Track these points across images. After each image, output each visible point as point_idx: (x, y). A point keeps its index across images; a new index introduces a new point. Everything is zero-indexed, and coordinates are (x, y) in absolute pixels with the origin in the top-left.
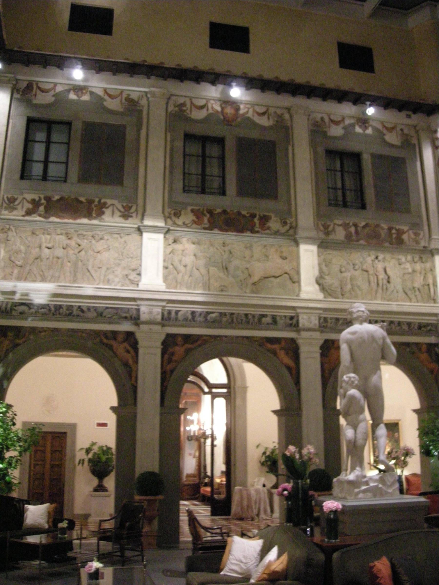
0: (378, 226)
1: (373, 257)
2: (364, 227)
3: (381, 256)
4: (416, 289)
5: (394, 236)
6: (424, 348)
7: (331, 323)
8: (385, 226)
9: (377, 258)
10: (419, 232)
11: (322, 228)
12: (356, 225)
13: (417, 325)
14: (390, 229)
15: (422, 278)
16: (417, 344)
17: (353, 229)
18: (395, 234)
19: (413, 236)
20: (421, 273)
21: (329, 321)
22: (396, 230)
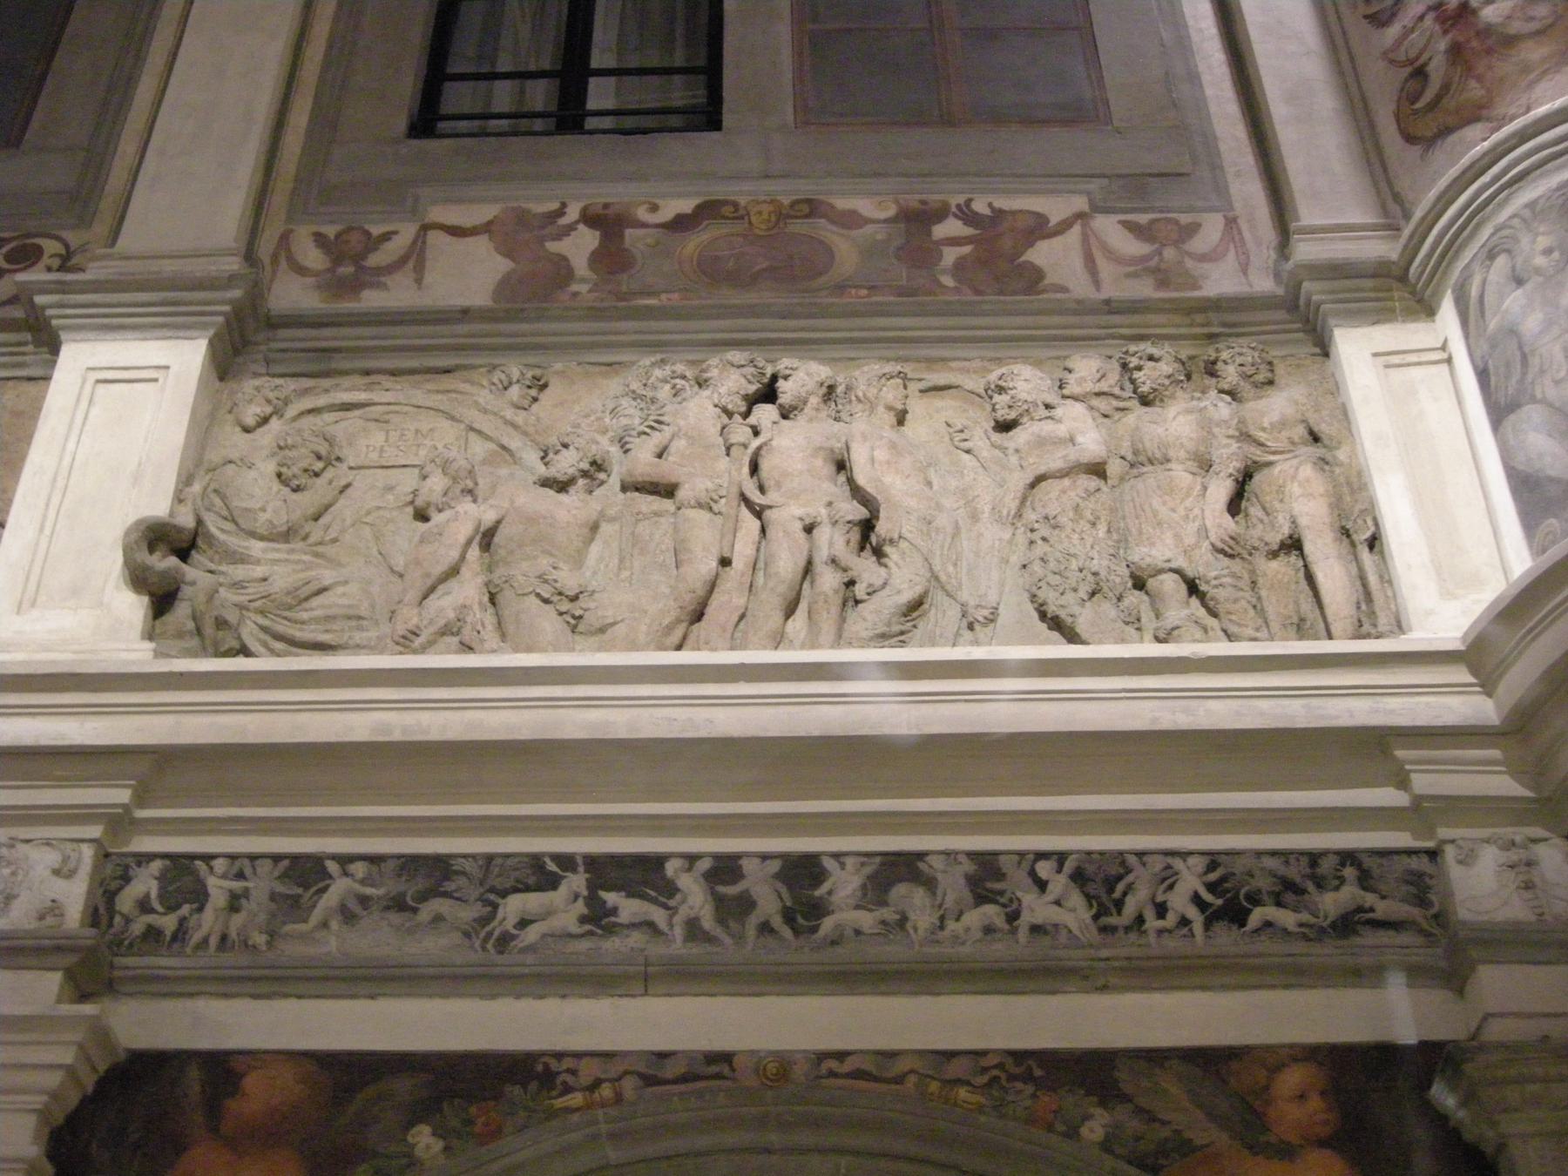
0: (812, 208)
1: (732, 382)
2: (680, 224)
3: (802, 376)
4: (1170, 585)
5: (950, 255)
6: (1297, 1104)
7: (235, 903)
8: (873, 206)
9: (768, 394)
10: (1185, 219)
11: (314, 258)
12: (608, 223)
13: (1191, 880)
14: (918, 219)
15: (1221, 490)
16: (1210, 1062)
17: (580, 246)
18: (954, 241)
19: (1133, 247)
20: (1205, 465)
21: (218, 888)
22: (969, 217)
